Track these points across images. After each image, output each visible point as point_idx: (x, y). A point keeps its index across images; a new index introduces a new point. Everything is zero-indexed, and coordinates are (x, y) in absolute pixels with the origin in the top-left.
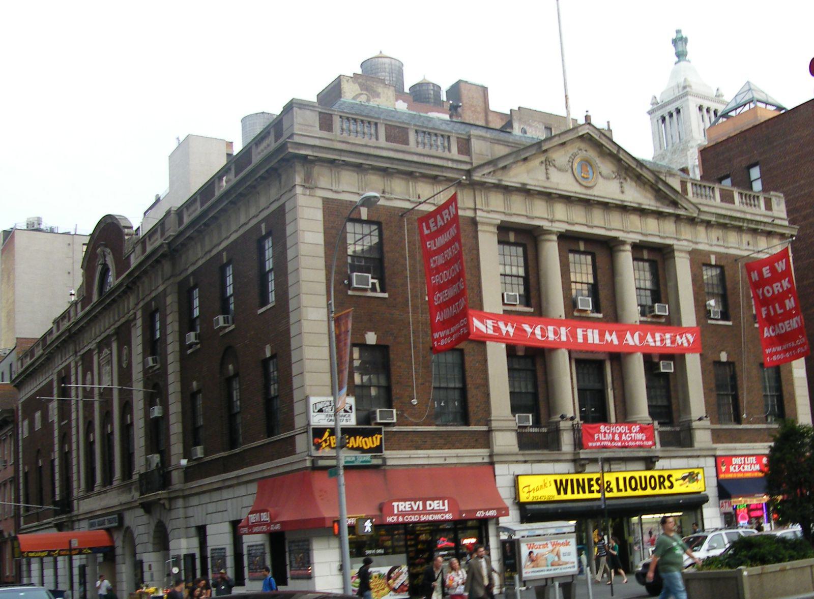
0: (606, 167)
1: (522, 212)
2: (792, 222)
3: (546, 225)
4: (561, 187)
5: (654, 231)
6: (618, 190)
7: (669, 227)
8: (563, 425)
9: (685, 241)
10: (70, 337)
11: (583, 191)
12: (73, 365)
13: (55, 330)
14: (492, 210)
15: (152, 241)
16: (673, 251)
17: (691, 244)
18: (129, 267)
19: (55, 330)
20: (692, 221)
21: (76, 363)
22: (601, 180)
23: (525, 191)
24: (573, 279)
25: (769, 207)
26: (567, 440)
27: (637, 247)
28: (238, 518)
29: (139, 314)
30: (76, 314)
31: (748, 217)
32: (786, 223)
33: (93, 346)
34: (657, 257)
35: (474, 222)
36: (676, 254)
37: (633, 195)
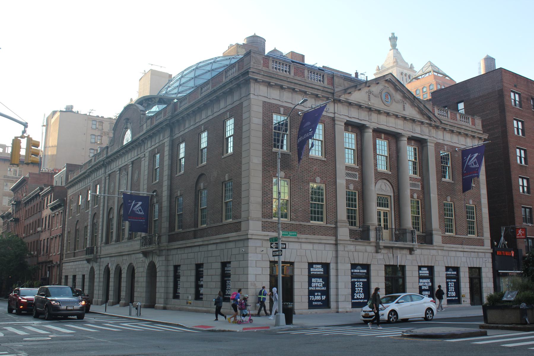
0: (398, 96)
1: (356, 116)
2: (484, 132)
3: (367, 123)
4: (375, 105)
5: (418, 131)
6: (402, 109)
7: (426, 129)
8: (371, 228)
9: (434, 137)
10: (103, 165)
11: (386, 108)
12: (103, 178)
13: (93, 160)
14: (343, 114)
15: (157, 118)
16: (427, 142)
17: (435, 139)
18: (143, 131)
19: (93, 160)
20: (437, 127)
21: (105, 178)
22: (394, 103)
23: (359, 106)
24: (378, 153)
25: (474, 124)
26: (372, 234)
27: (411, 139)
28: (202, 262)
29: (147, 155)
30: (107, 153)
31: (464, 127)
32: (482, 132)
33: (117, 169)
34: (420, 143)
35: (333, 119)
36: (428, 144)
37: (411, 112)
